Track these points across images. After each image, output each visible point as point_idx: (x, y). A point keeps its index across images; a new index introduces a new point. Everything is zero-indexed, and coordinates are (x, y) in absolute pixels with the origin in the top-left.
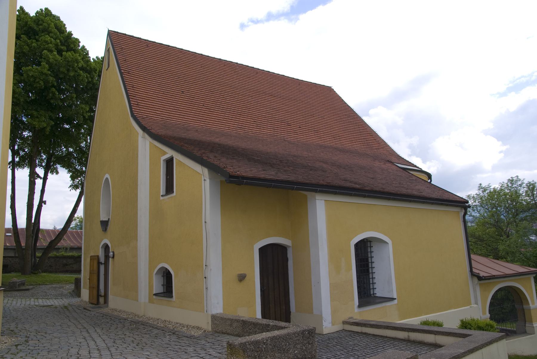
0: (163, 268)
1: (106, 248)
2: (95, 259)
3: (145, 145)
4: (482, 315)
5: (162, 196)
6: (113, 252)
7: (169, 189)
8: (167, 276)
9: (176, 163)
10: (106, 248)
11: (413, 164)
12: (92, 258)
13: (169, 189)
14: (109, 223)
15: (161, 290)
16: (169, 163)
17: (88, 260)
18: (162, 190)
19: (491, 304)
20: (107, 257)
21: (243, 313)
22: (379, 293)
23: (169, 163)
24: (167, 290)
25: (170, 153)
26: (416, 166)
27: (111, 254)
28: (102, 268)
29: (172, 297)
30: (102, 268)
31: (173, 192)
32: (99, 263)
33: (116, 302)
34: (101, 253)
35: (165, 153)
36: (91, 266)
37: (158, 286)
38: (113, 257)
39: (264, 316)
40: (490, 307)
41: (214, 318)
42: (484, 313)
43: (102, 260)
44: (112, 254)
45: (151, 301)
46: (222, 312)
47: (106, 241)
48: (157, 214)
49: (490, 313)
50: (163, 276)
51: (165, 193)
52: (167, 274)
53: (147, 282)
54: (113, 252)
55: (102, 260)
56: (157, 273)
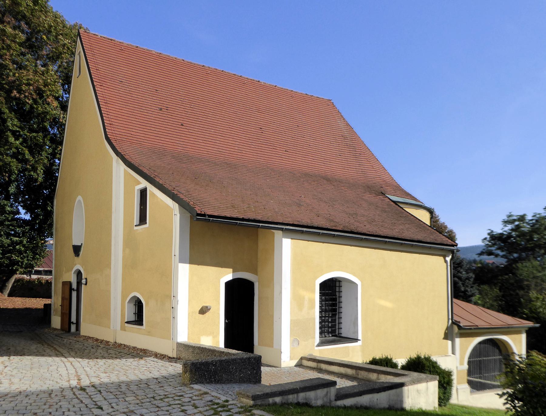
0: (135, 297)
1: (79, 274)
2: (67, 285)
3: (119, 169)
4: (458, 365)
5: (136, 226)
6: (86, 279)
7: (143, 220)
8: (139, 305)
9: (150, 194)
10: (79, 274)
11: (413, 197)
12: (64, 283)
13: (143, 220)
14: (82, 249)
15: (133, 318)
16: (143, 193)
17: (61, 285)
18: (136, 220)
19: (472, 355)
20: (79, 283)
21: (207, 342)
22: (345, 332)
23: (143, 193)
24: (139, 320)
25: (144, 183)
26: (415, 199)
27: (84, 281)
28: (74, 294)
29: (142, 325)
30: (74, 294)
31: (146, 223)
32: (71, 289)
33: (88, 329)
34: (73, 279)
35: (139, 183)
36: (63, 293)
37: (130, 313)
38: (86, 284)
39: (226, 346)
40: (469, 358)
41: (179, 345)
42: (462, 363)
43: (74, 286)
44: (85, 280)
45: (123, 329)
46: (187, 340)
47: (78, 267)
48: (130, 241)
49: (469, 363)
50: (135, 305)
51: (138, 223)
52: (138, 303)
53: (119, 309)
54: (86, 279)
55: (74, 286)
56: (129, 302)
